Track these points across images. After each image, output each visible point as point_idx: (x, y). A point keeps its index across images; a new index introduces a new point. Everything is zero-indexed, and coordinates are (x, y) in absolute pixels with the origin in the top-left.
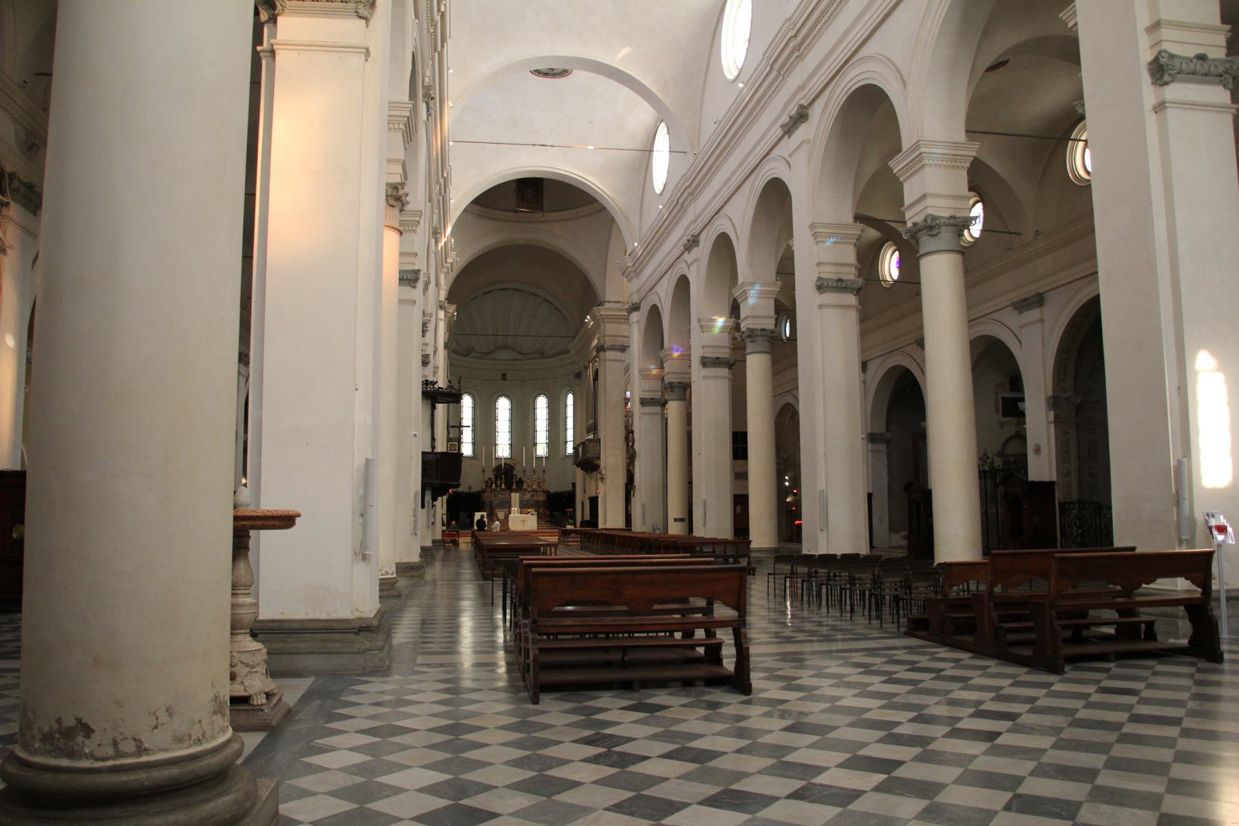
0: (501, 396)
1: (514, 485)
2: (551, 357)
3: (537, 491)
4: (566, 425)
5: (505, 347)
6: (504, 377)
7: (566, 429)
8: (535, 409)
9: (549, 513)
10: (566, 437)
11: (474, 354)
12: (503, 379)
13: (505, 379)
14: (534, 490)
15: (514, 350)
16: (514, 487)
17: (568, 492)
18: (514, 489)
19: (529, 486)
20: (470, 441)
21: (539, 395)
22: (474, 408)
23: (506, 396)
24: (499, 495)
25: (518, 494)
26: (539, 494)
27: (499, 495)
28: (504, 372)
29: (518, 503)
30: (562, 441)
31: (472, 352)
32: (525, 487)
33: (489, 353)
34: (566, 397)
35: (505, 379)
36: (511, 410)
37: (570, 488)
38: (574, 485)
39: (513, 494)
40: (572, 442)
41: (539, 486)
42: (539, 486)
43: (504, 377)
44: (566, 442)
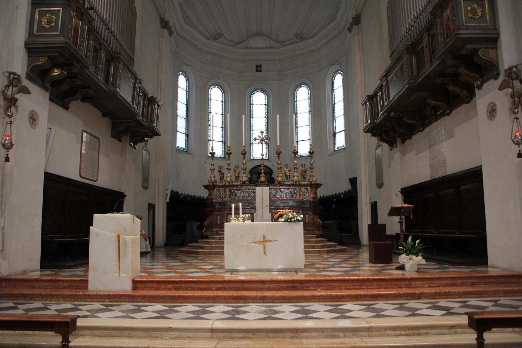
0: (257, 90)
1: (263, 175)
2: (312, 37)
3: (300, 185)
4: (333, 113)
5: (259, 34)
6: (259, 68)
7: (334, 119)
8: (295, 101)
9: (320, 221)
10: (334, 128)
11: (222, 39)
12: (257, 71)
13: (260, 71)
14: (295, 184)
15: (269, 37)
16: (263, 179)
17: (346, 193)
18: (262, 182)
19: (287, 177)
20: (220, 139)
21: (299, 86)
22: (224, 102)
23: (262, 90)
24: (238, 193)
25: (266, 189)
26: (303, 189)
27: (238, 193)
28: (259, 63)
29: (268, 203)
30: (329, 134)
31: (220, 37)
32: (280, 179)
33: (241, 42)
34: (333, 80)
35: (260, 71)
36: (268, 105)
37: (345, 187)
38: (353, 182)
39: (258, 189)
40: (343, 133)
41: (304, 177)
42: (304, 177)
43: (259, 68)
44: (334, 134)
